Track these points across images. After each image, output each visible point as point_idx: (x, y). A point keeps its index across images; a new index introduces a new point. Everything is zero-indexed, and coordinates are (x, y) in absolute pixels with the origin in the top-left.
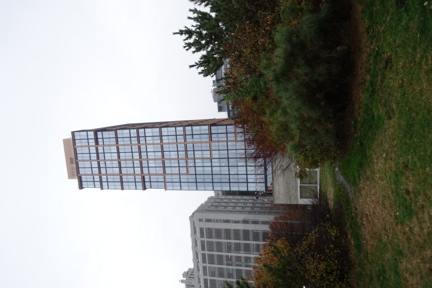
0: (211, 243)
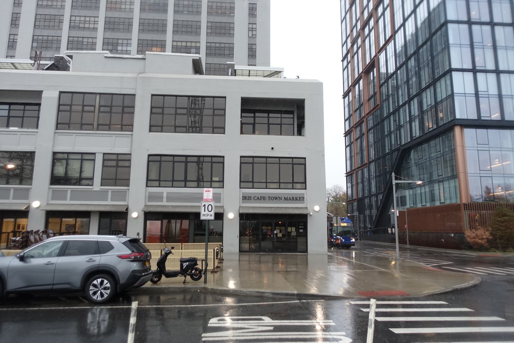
0: (195, 10)
